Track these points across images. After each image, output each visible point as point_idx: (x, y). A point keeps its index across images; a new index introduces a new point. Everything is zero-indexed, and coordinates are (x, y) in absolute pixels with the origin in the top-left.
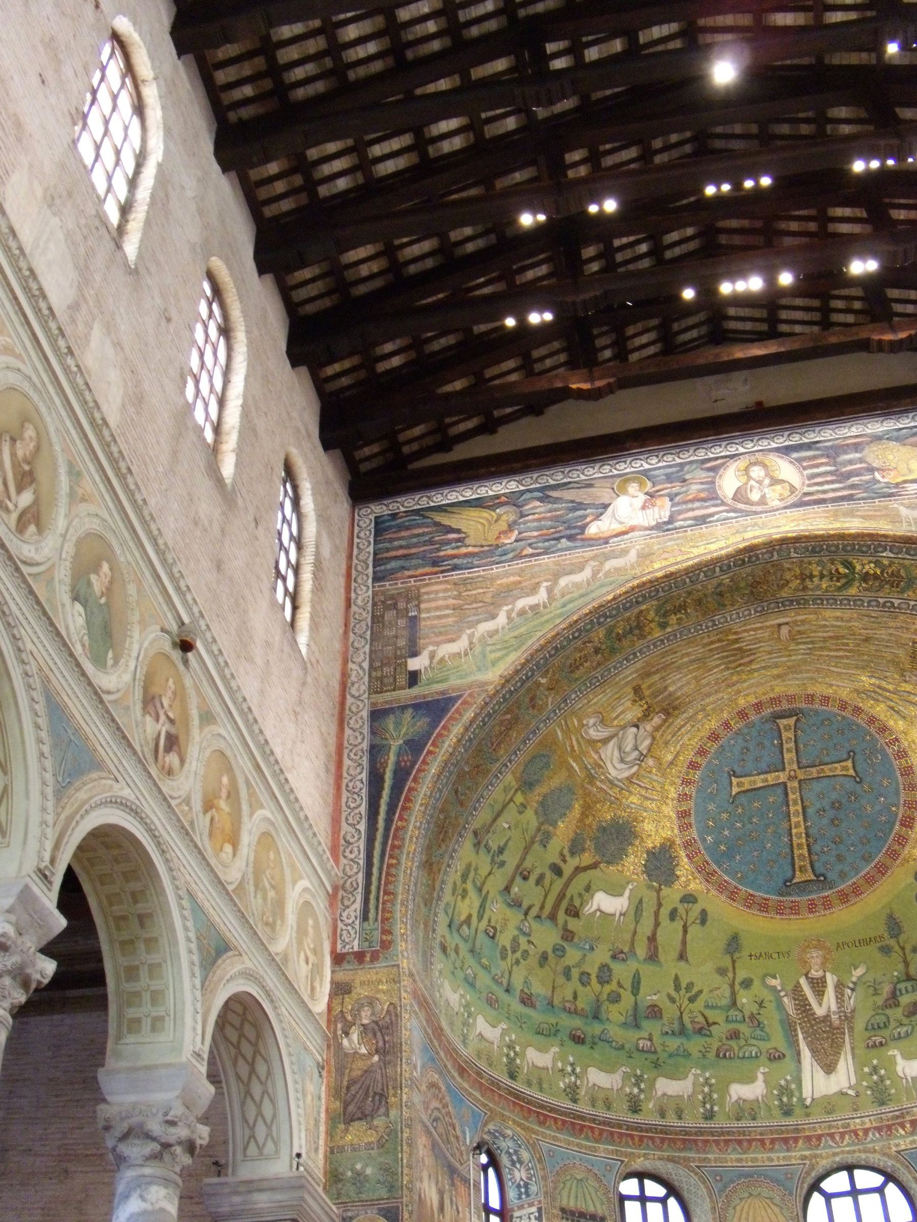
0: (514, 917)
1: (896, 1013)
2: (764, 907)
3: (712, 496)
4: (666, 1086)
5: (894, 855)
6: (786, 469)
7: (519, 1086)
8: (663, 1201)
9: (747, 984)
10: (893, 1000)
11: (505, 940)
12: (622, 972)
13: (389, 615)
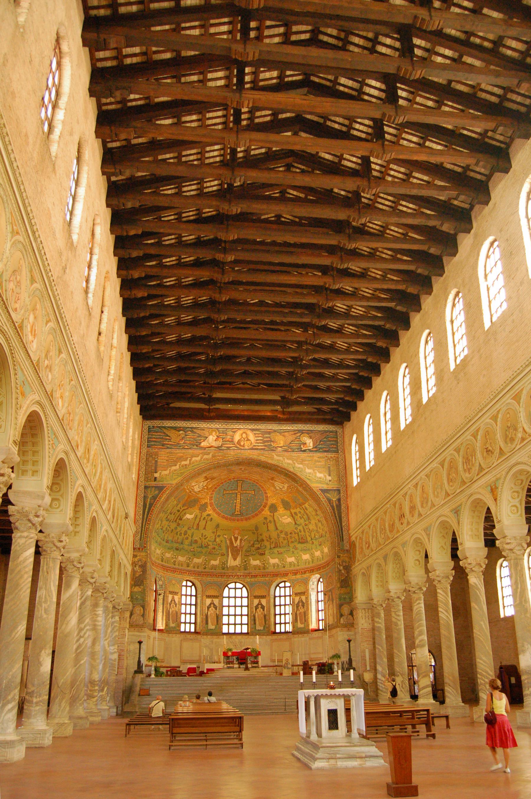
0: (167, 523)
1: (254, 548)
2: (226, 519)
3: (232, 441)
4: (196, 560)
5: (260, 512)
6: (251, 437)
7: (164, 563)
8: (191, 587)
9: (219, 536)
10: (253, 545)
11: (164, 529)
12: (190, 532)
13: (151, 459)
